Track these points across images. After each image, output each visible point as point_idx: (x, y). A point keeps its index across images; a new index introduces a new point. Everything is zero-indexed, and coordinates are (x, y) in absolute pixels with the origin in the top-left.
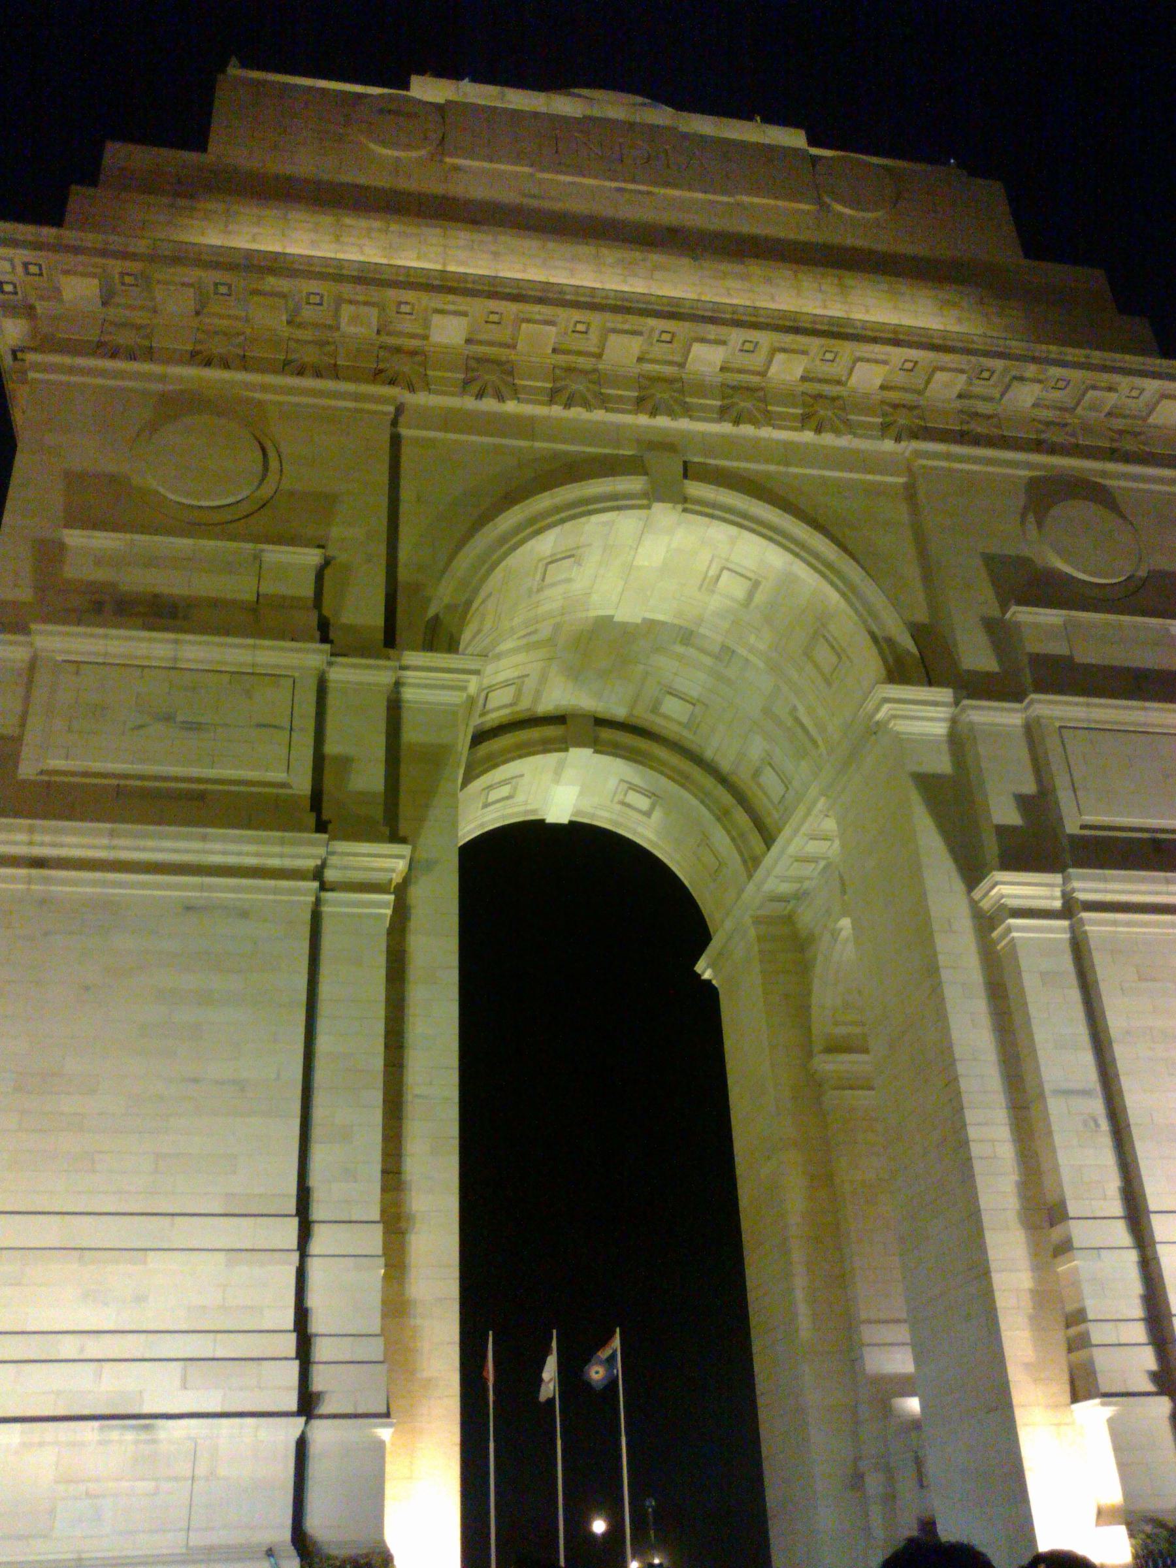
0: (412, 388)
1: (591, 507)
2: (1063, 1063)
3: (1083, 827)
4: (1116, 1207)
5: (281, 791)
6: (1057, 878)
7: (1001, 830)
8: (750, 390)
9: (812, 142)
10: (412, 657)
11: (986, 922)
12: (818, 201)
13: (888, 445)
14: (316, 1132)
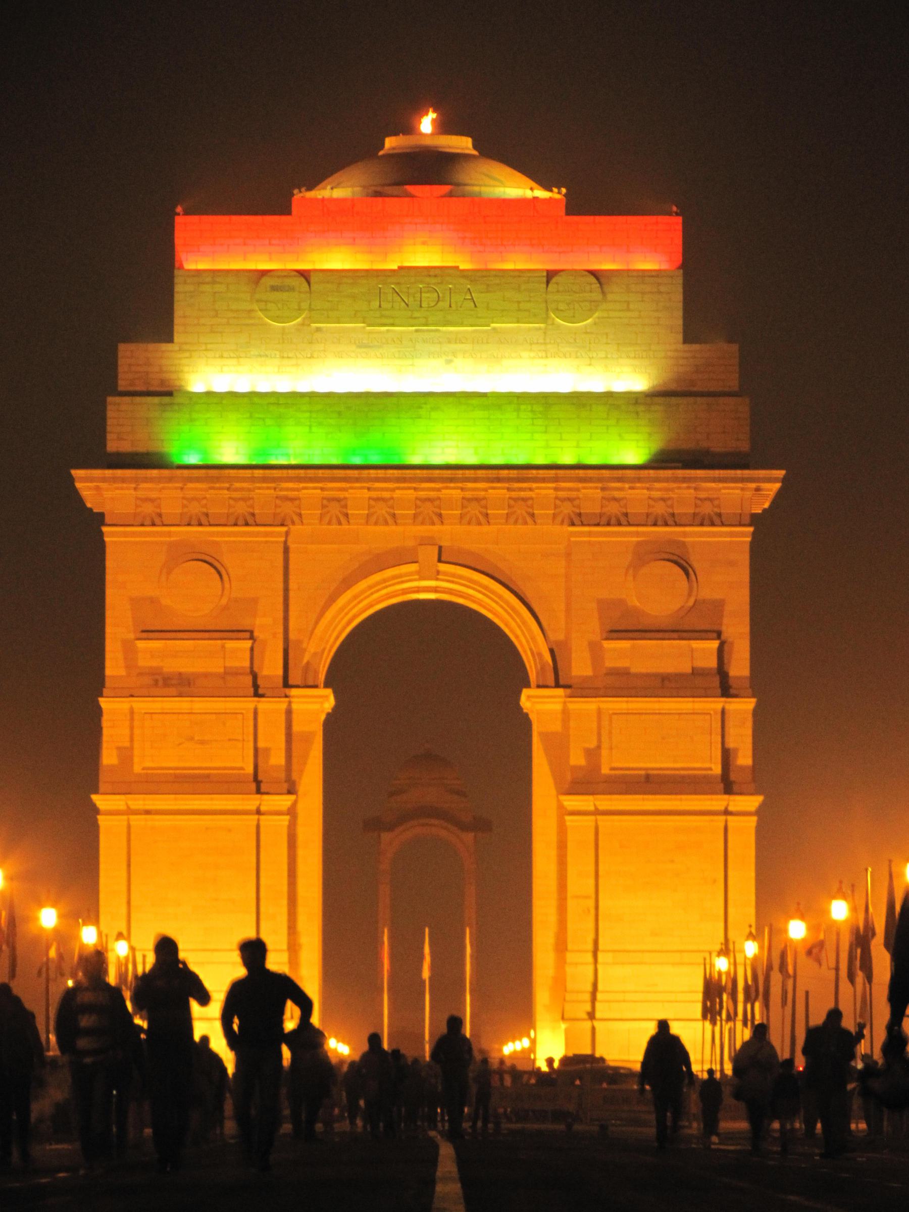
0: (293, 523)
1: (387, 584)
2: (579, 883)
3: (612, 769)
4: (590, 946)
5: (242, 772)
6: (591, 798)
8: (477, 500)
10: (294, 692)
11: (563, 812)
12: (546, 319)
14: (262, 916)
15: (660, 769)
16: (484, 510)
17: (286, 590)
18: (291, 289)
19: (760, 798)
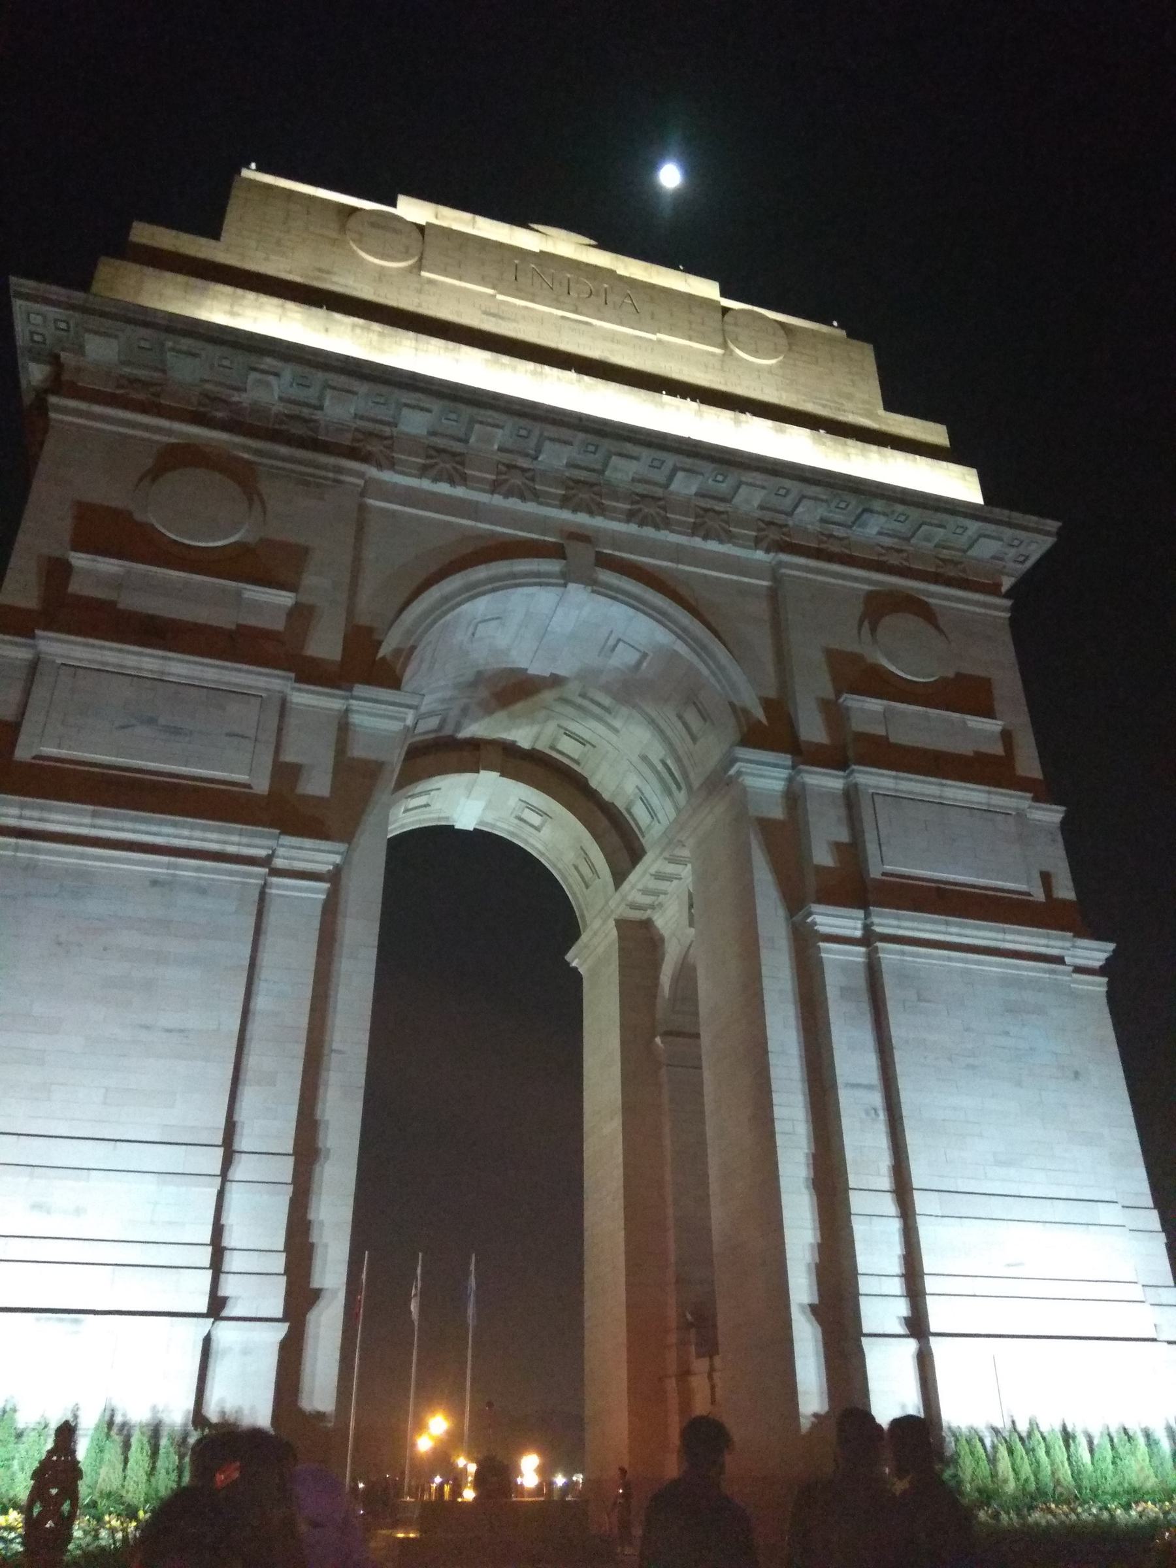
0: (380, 466)
1: (518, 581)
2: (854, 1061)
3: (884, 874)
4: (885, 1181)
5: (247, 790)
7: (820, 870)
9: (724, 293)
12: (724, 346)
13: (760, 555)
15: (956, 884)
16: (662, 512)
17: (357, 560)
18: (396, 231)
19: (1111, 946)
